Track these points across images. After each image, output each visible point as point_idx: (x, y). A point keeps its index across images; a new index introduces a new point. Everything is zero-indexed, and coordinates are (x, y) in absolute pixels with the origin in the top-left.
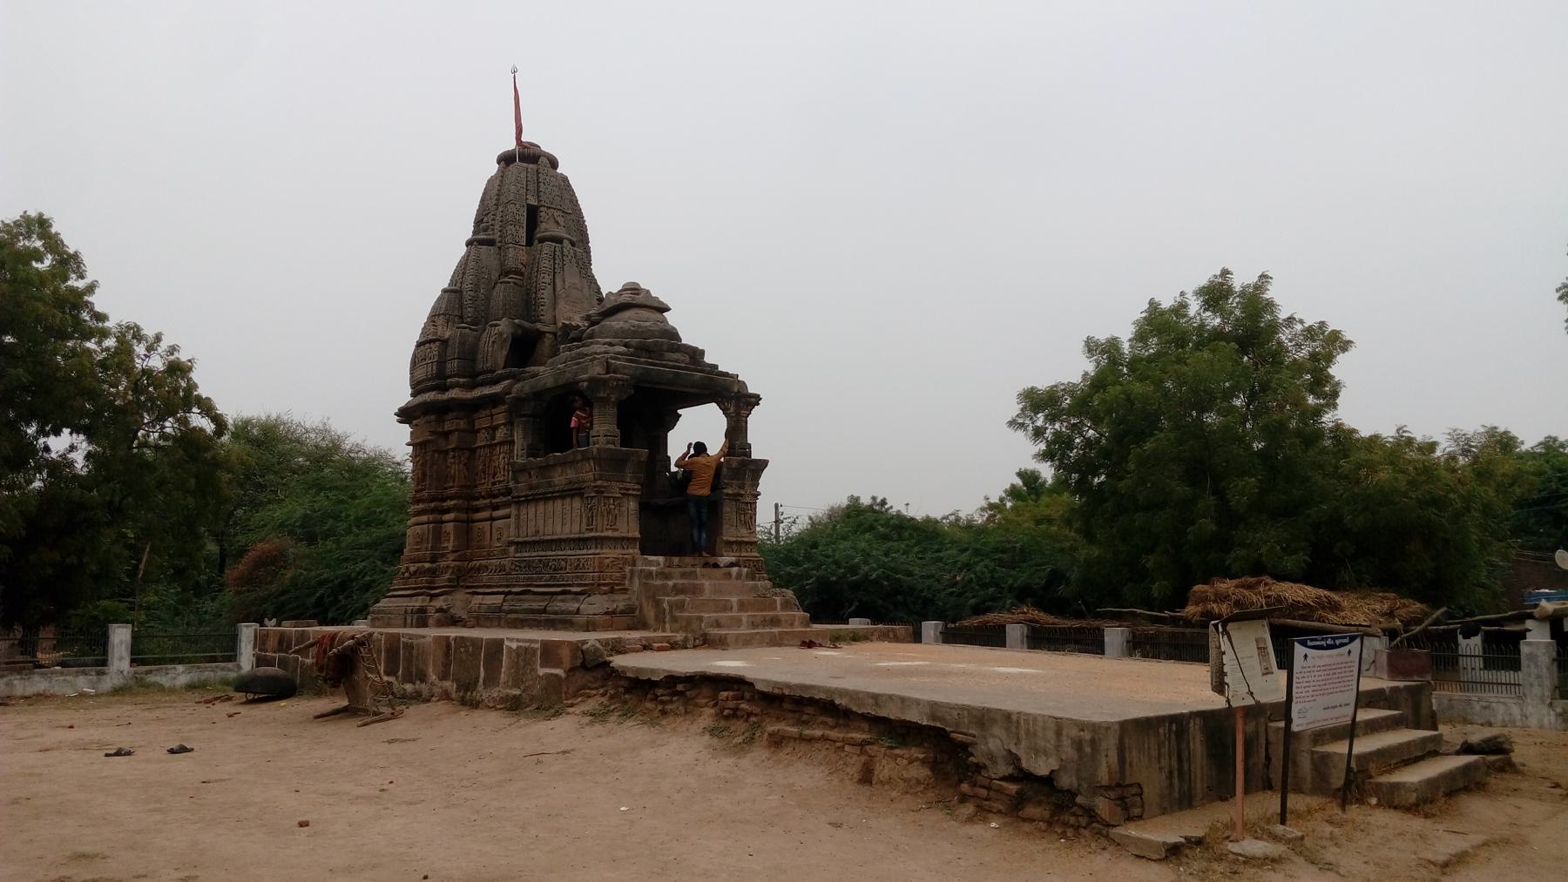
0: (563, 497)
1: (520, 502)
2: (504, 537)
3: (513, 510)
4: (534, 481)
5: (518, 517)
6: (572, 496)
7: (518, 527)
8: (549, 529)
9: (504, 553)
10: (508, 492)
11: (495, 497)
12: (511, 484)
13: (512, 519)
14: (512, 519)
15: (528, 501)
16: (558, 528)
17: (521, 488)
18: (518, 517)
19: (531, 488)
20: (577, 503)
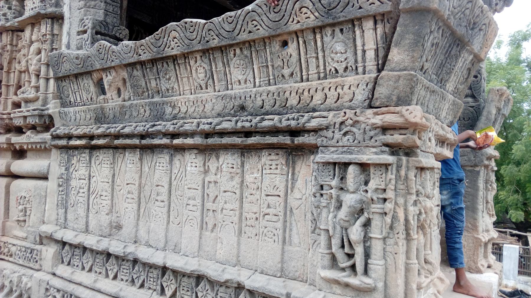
0: (203, 150)
1: (67, 146)
2: (33, 219)
3: (53, 164)
4: (112, 102)
5: (65, 182)
6: (245, 151)
7: (64, 204)
8: (155, 227)
9: (31, 258)
10: (47, 124)
11: (19, 131)
12: (53, 108)
13: (52, 185)
14: (52, 185)
15: (91, 146)
16: (189, 236)
17: (76, 118)
18: (65, 182)
19: (100, 118)
20: (267, 172)
